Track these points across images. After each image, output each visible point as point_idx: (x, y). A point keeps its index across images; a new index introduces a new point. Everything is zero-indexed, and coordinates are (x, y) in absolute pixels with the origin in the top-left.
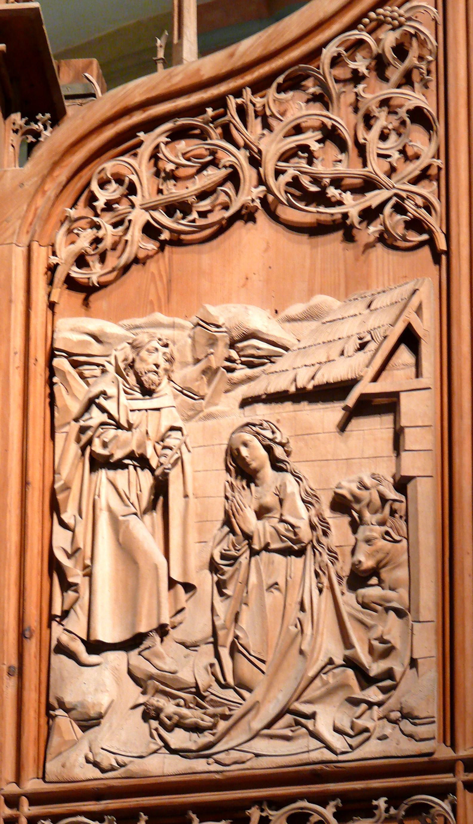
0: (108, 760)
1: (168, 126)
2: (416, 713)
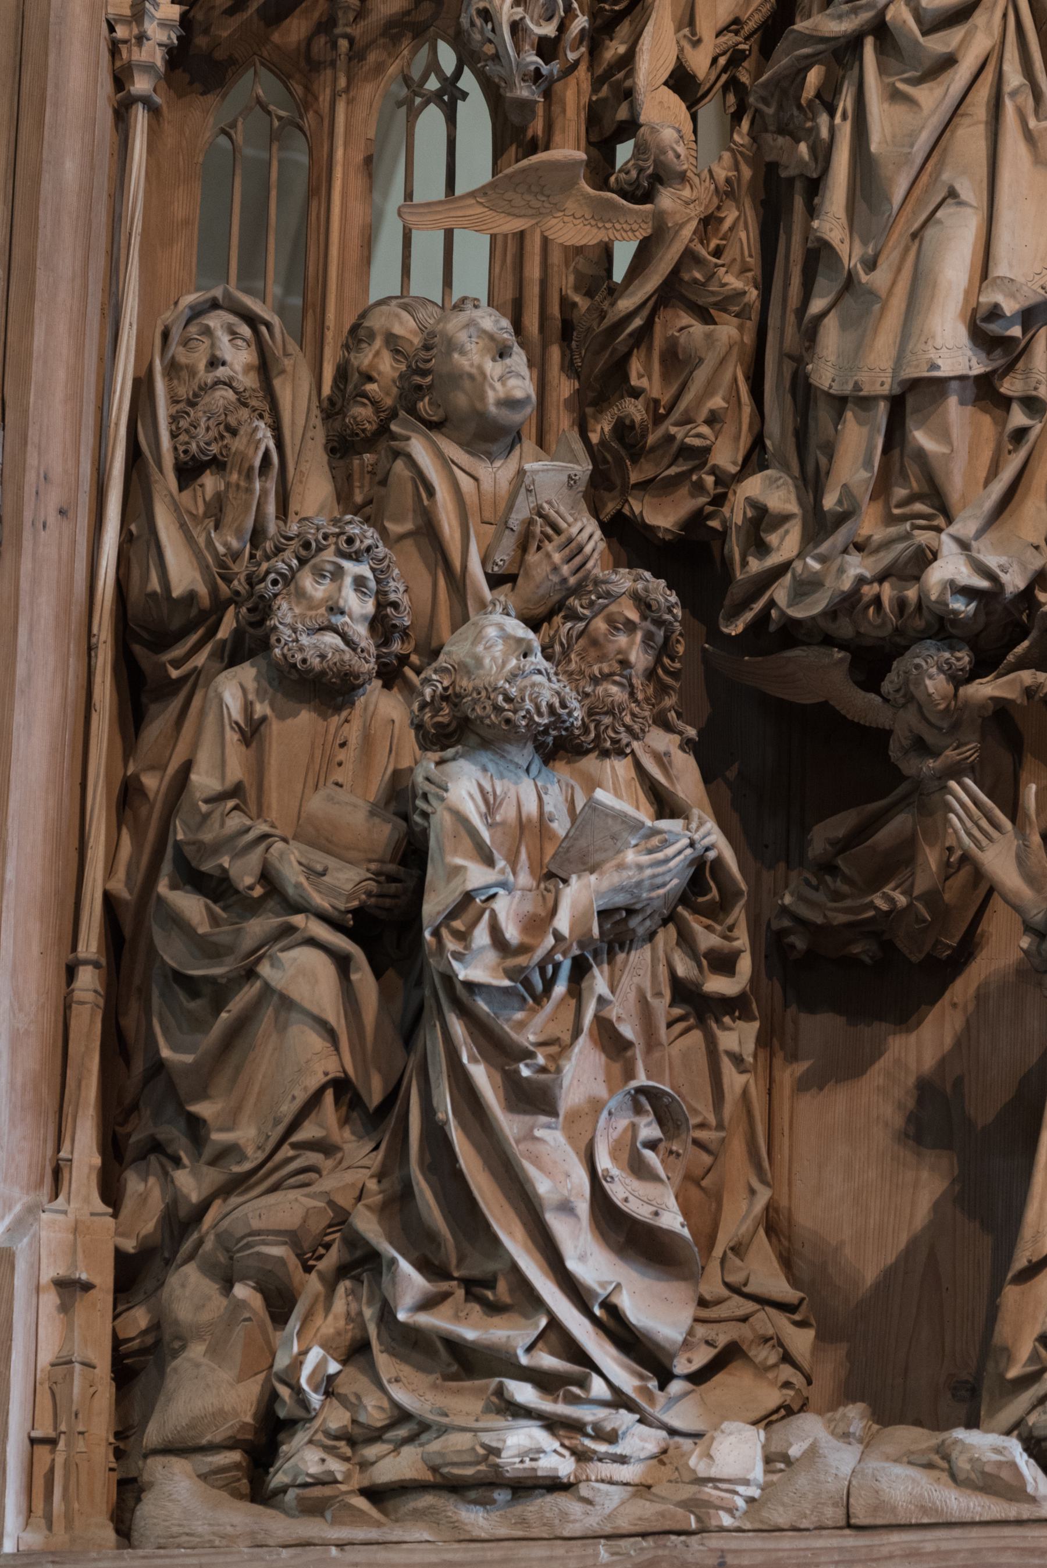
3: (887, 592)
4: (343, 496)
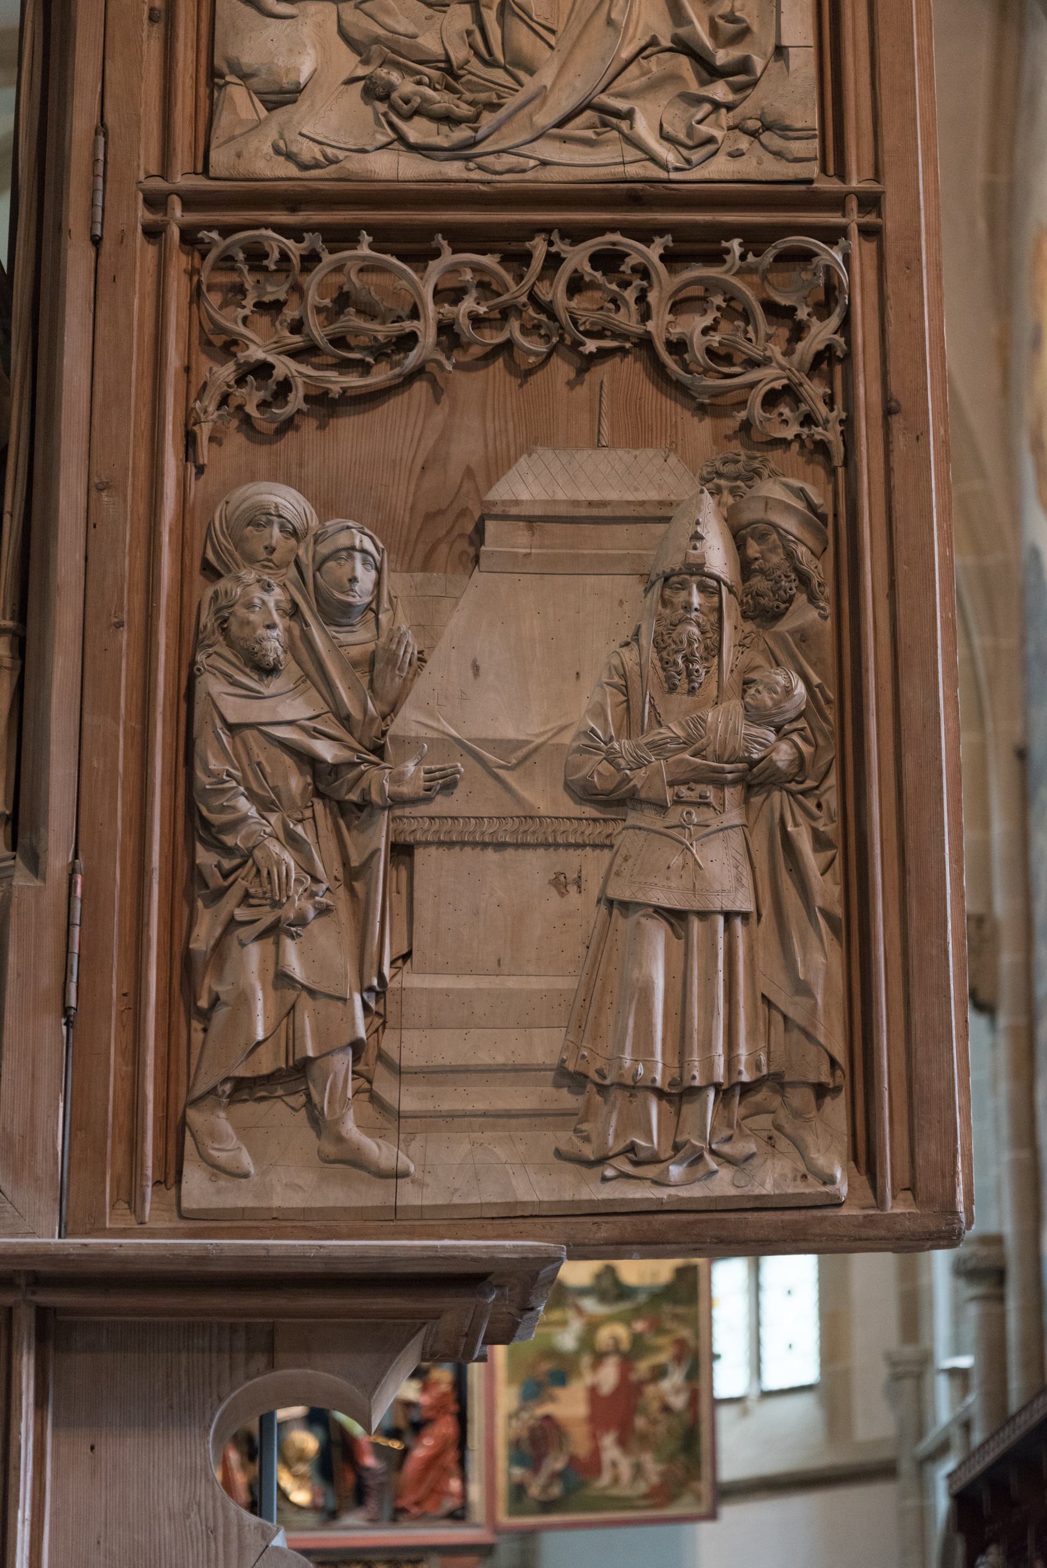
2: (788, 122)
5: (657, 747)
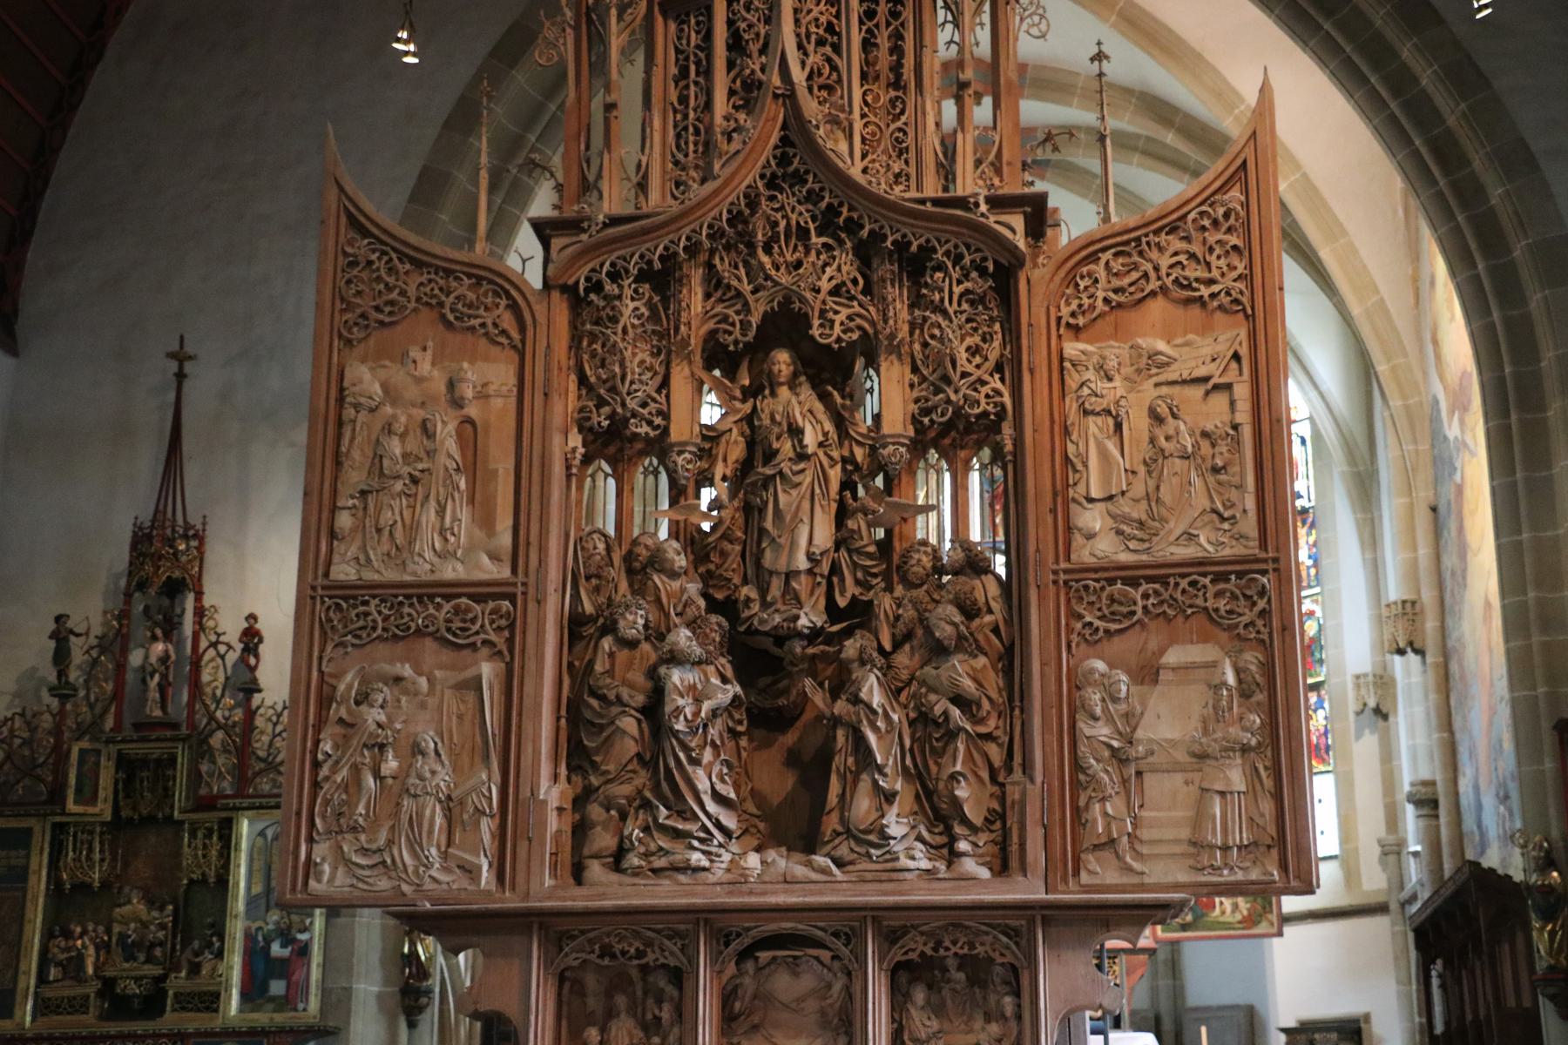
0: (1100, 554)
1: (1113, 251)
3: (785, 624)
4: (631, 585)
5: (1215, 740)
